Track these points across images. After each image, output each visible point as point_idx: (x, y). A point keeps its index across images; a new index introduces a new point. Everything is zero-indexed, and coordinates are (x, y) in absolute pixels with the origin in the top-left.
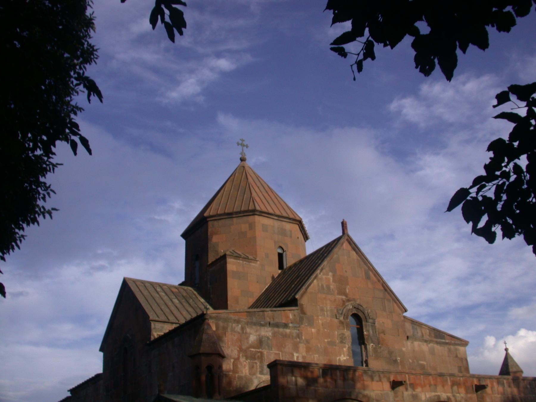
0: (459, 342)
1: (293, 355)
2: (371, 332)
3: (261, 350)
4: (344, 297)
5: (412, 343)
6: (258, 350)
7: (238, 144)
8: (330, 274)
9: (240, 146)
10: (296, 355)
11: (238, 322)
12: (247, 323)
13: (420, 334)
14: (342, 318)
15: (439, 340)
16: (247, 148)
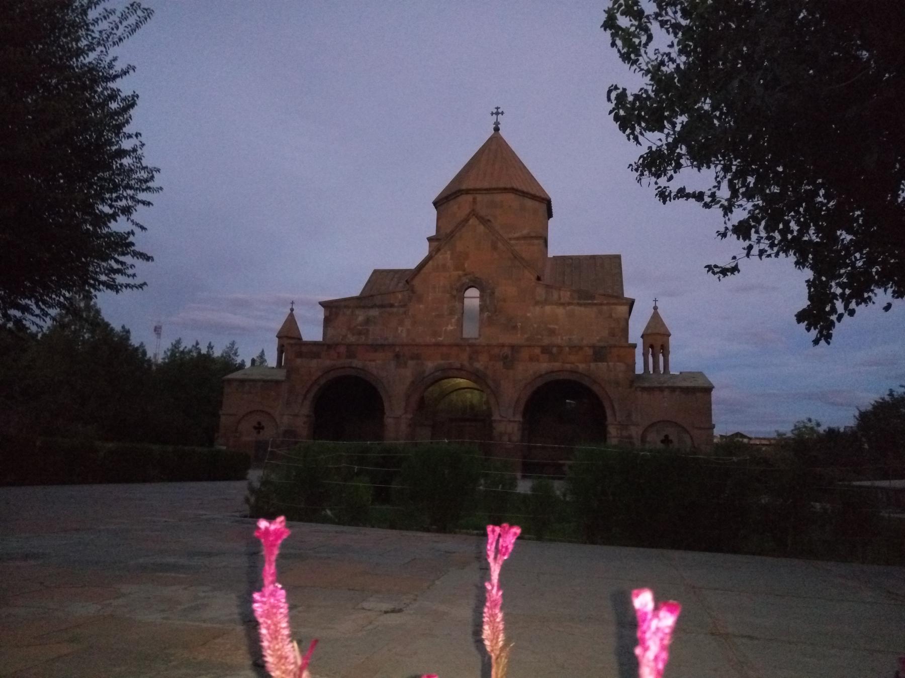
0: (615, 301)
1: (397, 329)
2: (488, 302)
3: (367, 327)
4: (461, 273)
5: (542, 307)
6: (364, 327)
7: (492, 114)
8: (449, 252)
9: (494, 115)
10: (399, 328)
11: (346, 307)
12: (357, 307)
13: (556, 296)
14: (455, 293)
15: (582, 302)
16: (502, 115)
